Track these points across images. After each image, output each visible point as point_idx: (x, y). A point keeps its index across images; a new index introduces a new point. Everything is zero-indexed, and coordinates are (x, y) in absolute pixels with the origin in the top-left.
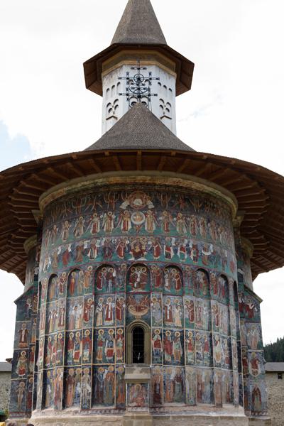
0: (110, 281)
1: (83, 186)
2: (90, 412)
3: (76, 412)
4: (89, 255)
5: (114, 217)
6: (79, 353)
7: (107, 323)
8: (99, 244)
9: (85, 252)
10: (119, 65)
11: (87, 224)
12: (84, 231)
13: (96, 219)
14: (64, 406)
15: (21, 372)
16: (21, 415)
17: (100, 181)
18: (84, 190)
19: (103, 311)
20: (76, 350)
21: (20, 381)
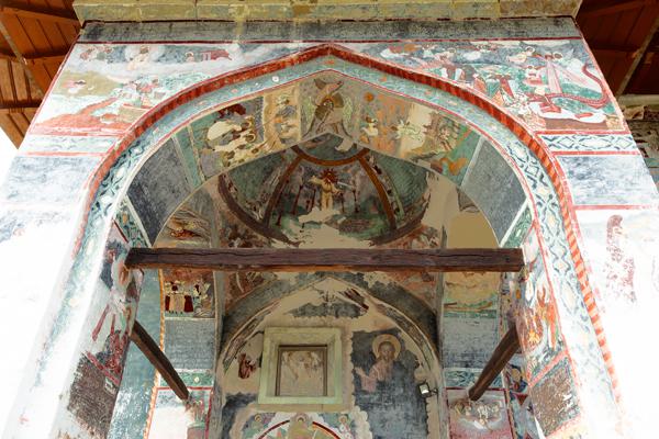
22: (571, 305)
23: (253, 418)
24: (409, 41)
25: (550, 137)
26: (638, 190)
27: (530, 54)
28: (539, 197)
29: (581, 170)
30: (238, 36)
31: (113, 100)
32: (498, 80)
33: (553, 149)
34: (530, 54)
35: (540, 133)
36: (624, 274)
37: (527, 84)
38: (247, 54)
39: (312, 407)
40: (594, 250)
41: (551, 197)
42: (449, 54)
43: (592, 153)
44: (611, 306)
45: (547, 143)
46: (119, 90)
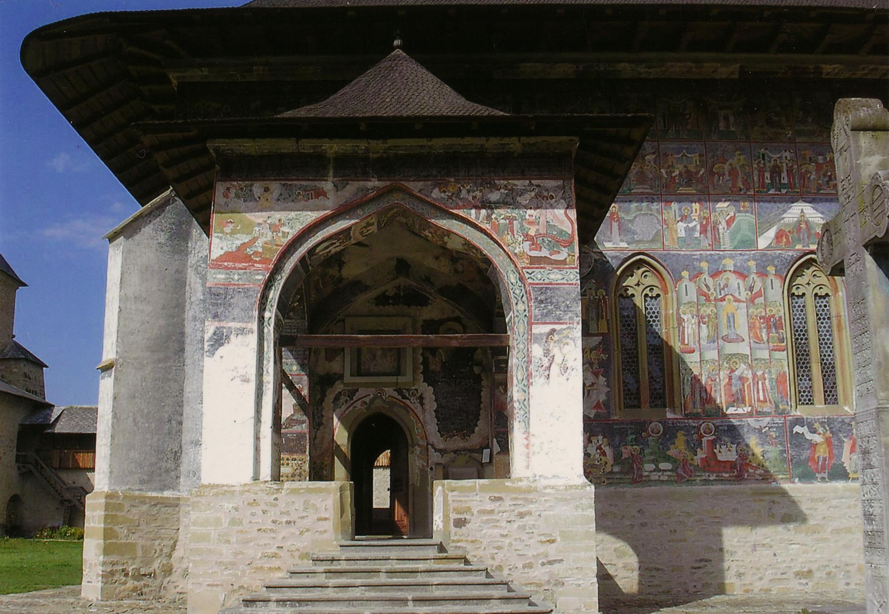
22: (520, 378)
23: (340, 393)
24: (452, 180)
25: (530, 271)
26: (571, 311)
27: (533, 194)
28: (518, 311)
29: (543, 297)
30: (331, 172)
31: (255, 239)
32: (507, 221)
33: (530, 281)
34: (533, 194)
35: (525, 268)
36: (547, 365)
37: (526, 225)
38: (339, 193)
39: (388, 385)
40: (537, 351)
41: (525, 311)
42: (478, 194)
43: (551, 284)
44: (538, 382)
45: (527, 276)
46: (257, 229)
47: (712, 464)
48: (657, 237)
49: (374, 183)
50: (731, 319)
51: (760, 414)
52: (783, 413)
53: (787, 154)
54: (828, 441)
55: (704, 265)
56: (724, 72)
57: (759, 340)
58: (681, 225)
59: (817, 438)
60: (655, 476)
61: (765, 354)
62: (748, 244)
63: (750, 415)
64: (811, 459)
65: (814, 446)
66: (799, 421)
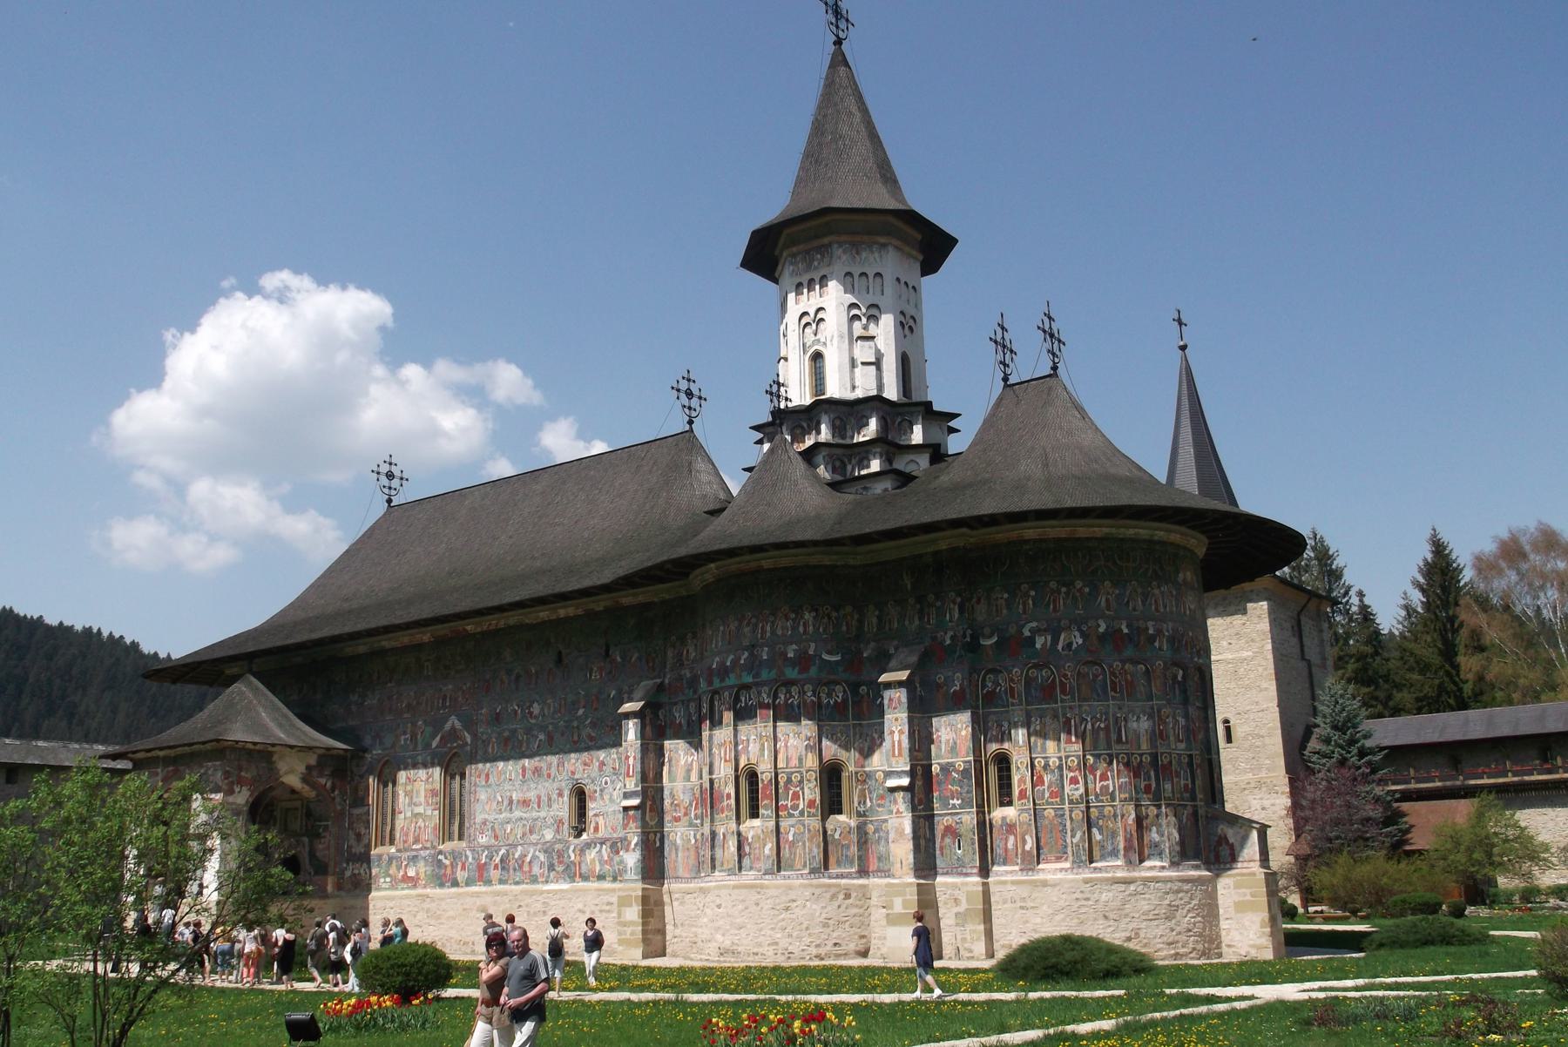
0: (1177, 686)
1: (1135, 534)
2: (1181, 868)
3: (1163, 868)
4: (1157, 644)
5: (1174, 593)
6: (1150, 785)
7: (1178, 744)
8: (1168, 628)
9: (1152, 639)
10: (882, 240)
11: (1145, 597)
12: (1144, 604)
13: (1156, 591)
14: (1141, 861)
15: (920, 802)
16: (926, 872)
17: (1160, 535)
18: (1133, 540)
19: (1173, 728)
20: (1145, 780)
21: (920, 817)
47: (406, 879)
48: (393, 746)
49: (171, 768)
50: (418, 792)
51: (426, 848)
52: (434, 847)
53: (450, 687)
54: (452, 864)
55: (410, 760)
56: (426, 638)
57: (428, 804)
58: (403, 737)
59: (447, 862)
60: (384, 885)
61: (429, 812)
62: (428, 745)
63: (421, 849)
64: (445, 875)
65: (446, 867)
66: (440, 852)
